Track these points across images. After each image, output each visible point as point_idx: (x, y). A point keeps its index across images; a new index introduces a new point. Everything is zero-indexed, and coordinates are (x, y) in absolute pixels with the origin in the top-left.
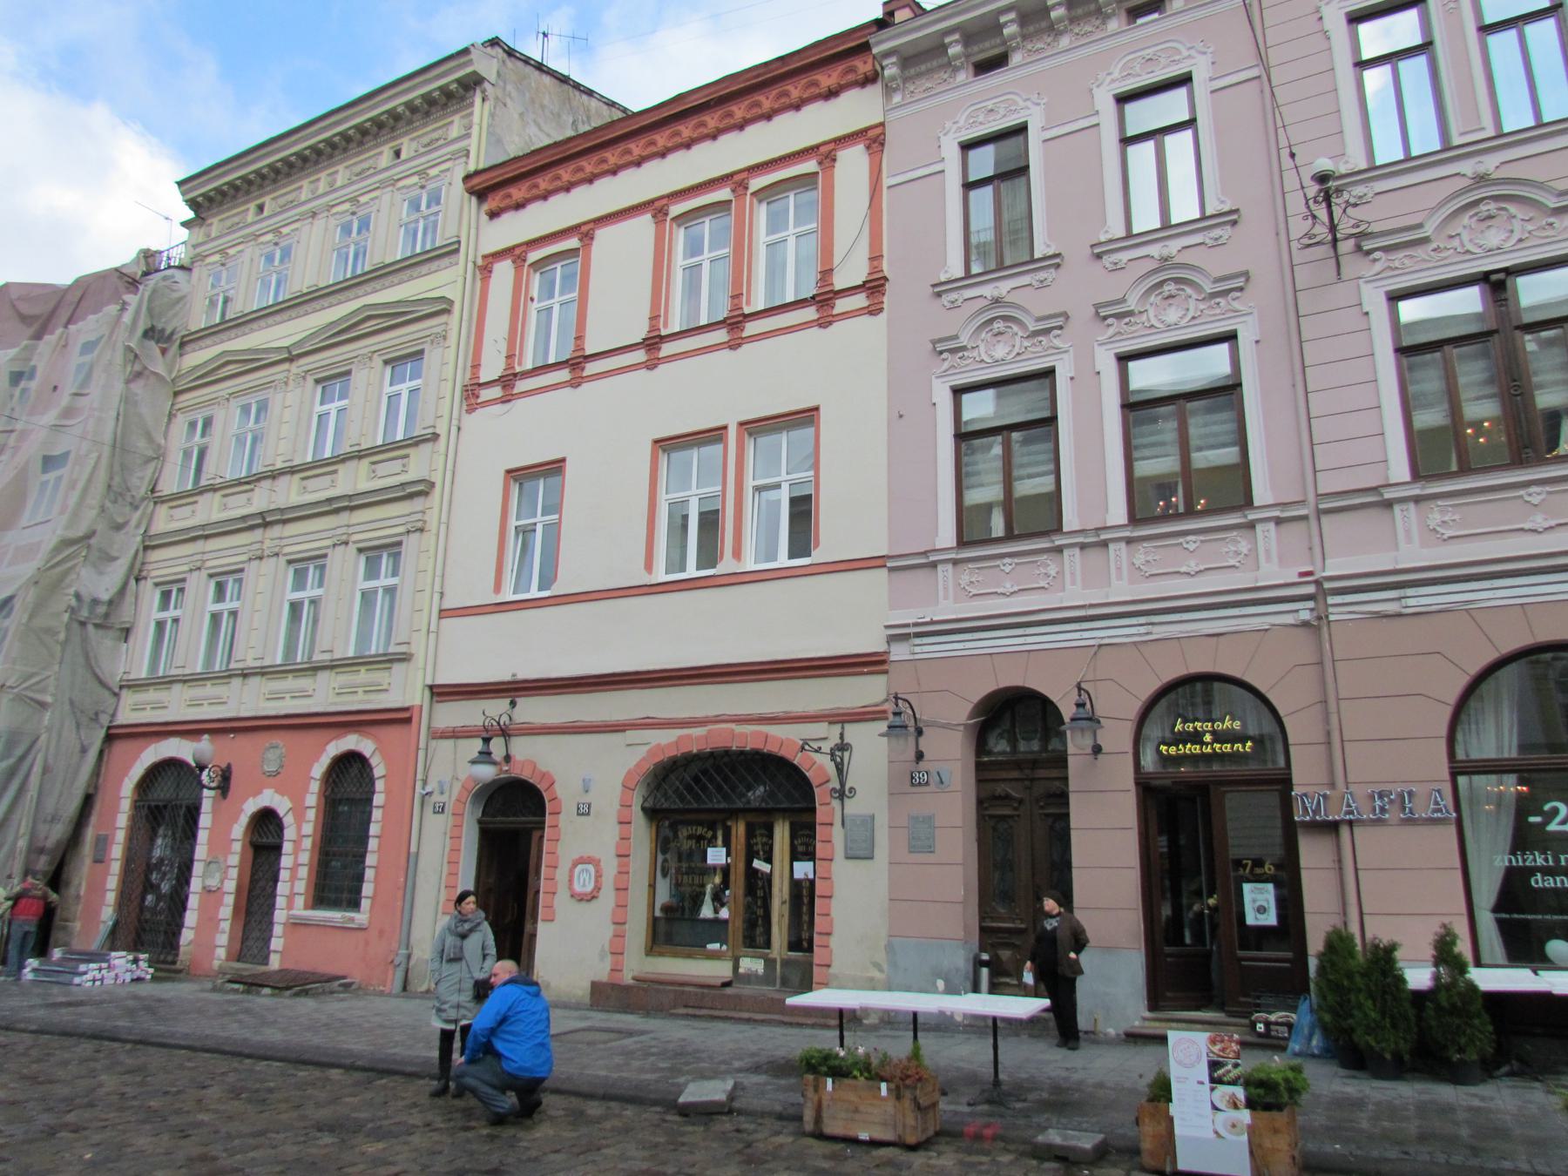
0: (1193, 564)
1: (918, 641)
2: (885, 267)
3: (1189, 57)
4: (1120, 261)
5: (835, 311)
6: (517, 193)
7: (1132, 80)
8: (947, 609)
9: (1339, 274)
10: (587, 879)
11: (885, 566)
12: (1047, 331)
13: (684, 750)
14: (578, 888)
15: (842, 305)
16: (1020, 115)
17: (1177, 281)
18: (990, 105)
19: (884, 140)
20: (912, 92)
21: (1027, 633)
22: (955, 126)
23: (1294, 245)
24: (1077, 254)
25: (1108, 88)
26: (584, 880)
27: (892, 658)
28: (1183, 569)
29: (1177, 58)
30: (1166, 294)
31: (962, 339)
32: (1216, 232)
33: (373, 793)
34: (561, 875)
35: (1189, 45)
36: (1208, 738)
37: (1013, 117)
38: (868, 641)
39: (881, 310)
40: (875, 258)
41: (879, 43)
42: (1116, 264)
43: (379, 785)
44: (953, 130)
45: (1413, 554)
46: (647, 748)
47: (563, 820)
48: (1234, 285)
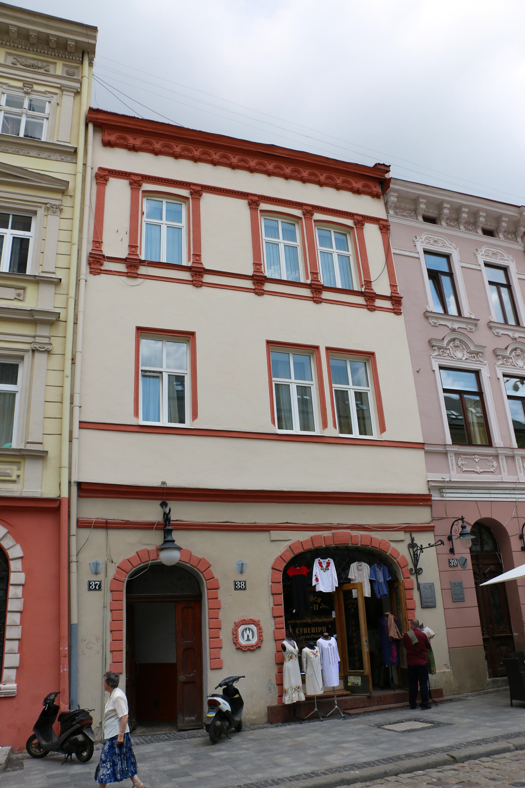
3: (507, 260)
6: (131, 141)
10: (250, 635)
11: (424, 448)
12: (477, 353)
13: (317, 545)
14: (243, 642)
20: (396, 213)
21: (473, 492)
22: (421, 240)
29: (504, 258)
33: (7, 570)
34: (225, 635)
37: (446, 249)
39: (401, 313)
40: (393, 286)
41: (394, 184)
42: (498, 333)
43: (15, 566)
46: (288, 543)
47: (222, 594)
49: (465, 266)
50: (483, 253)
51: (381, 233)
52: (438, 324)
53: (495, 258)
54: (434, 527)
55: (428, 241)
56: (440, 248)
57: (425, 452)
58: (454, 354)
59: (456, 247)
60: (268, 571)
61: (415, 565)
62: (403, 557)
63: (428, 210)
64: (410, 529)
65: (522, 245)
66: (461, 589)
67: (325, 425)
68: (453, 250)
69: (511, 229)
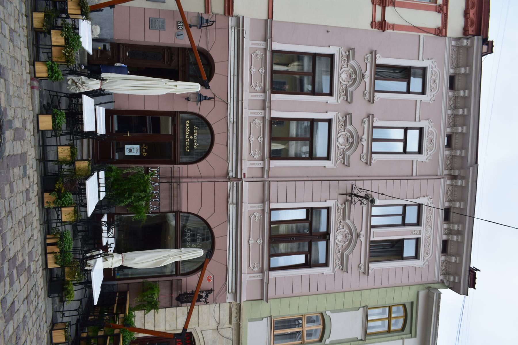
0: (253, 139)
1: (236, 30)
2: (389, 31)
3: (428, 154)
4: (365, 124)
5: (377, 6)
7: (427, 134)
8: (248, 44)
9: (341, 194)
12: (346, 95)
15: (379, 9)
17: (352, 143)
18: (437, 81)
19: (439, 36)
22: (434, 67)
23: (354, 182)
24: (372, 109)
25: (427, 126)
27: (230, 18)
28: (251, 136)
29: (429, 150)
30: (349, 139)
31: (352, 61)
32: (365, 157)
35: (431, 155)
36: (191, 137)
39: (372, 27)
40: (393, 27)
41: (478, 40)
42: (364, 122)
45: (247, 208)
48: (346, 162)
49: (417, 106)
50: (431, 129)
51: (436, 28)
52: (367, 62)
53: (428, 141)
54: (208, 12)
55: (434, 73)
56: (429, 86)
57: (266, 20)
58: (344, 72)
59: (432, 100)
63: (461, 58)
65: (442, 173)
66: (160, 28)
68: (429, 98)
69: (455, 165)
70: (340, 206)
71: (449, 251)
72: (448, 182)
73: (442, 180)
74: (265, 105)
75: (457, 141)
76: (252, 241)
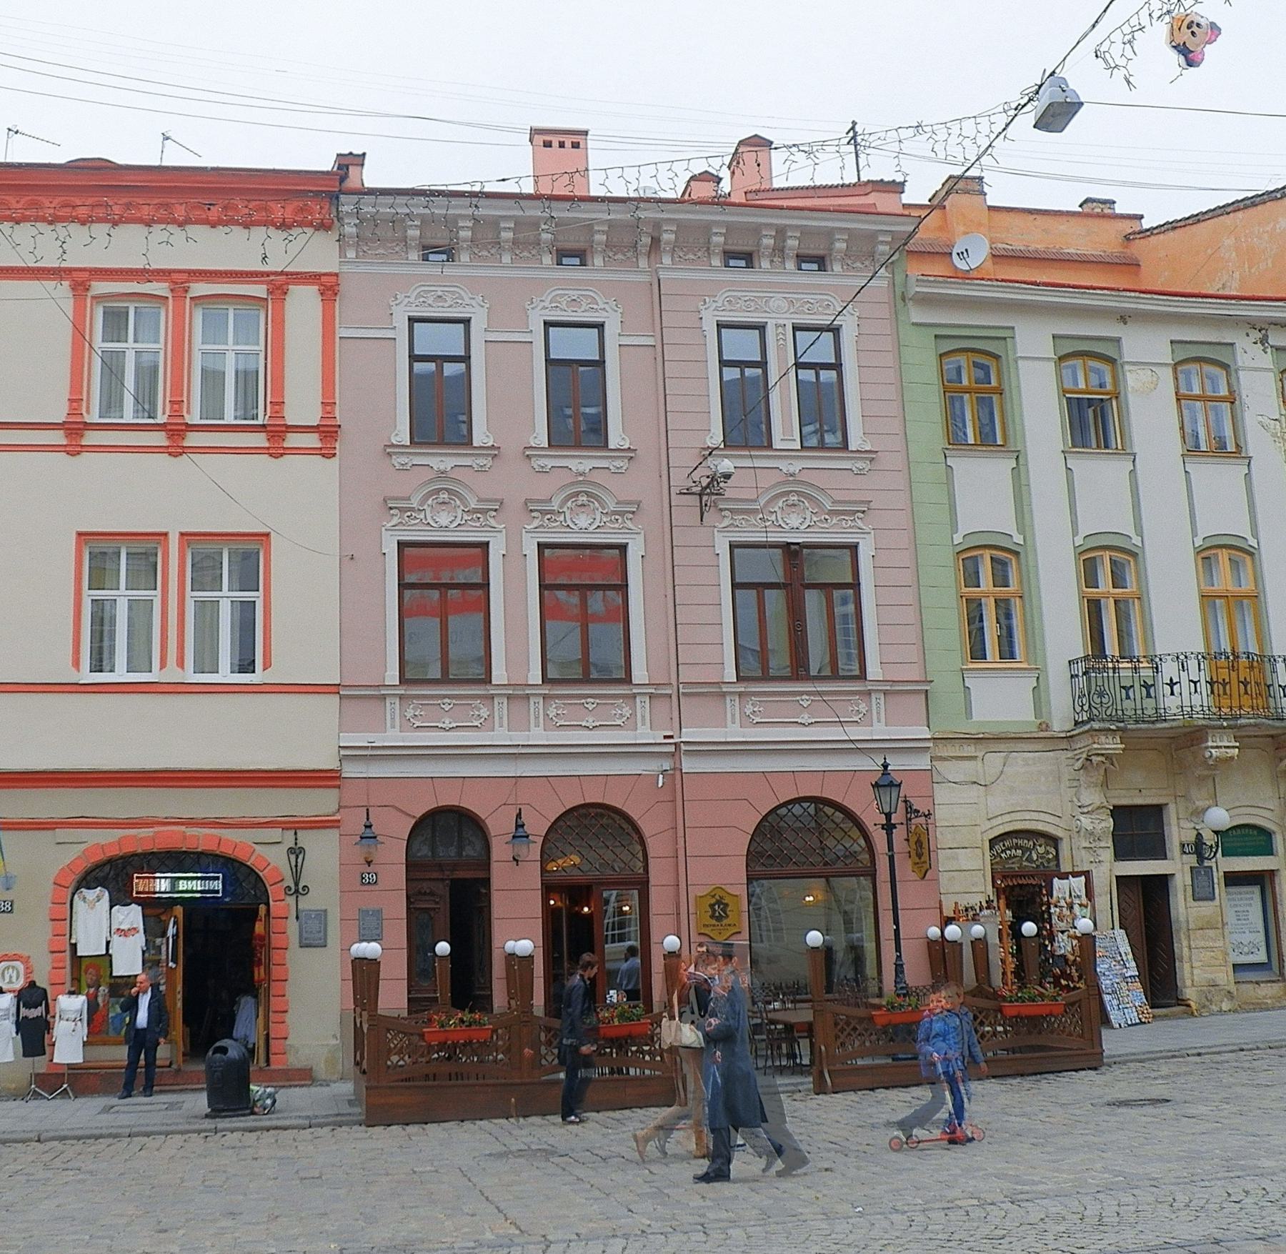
2: (337, 415)
7: (559, 313)
8: (393, 737)
15: (293, 440)
16: (464, 310)
22: (407, 300)
26: (11, 977)
27: (343, 775)
29: (595, 307)
32: (618, 463)
38: (324, 760)
39: (334, 455)
40: (328, 404)
44: (405, 303)
46: (83, 847)
48: (629, 510)
54: (339, 821)
55: (422, 300)
56: (450, 309)
60: (49, 887)
61: (297, 884)
62: (276, 869)
64: (295, 825)
67: (163, 665)
70: (726, 522)
71: (821, 252)
72: (667, 260)
73: (662, 275)
74: (518, 695)
75: (572, 238)
76: (805, 718)
